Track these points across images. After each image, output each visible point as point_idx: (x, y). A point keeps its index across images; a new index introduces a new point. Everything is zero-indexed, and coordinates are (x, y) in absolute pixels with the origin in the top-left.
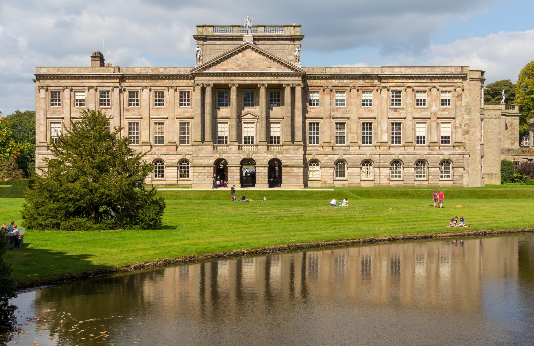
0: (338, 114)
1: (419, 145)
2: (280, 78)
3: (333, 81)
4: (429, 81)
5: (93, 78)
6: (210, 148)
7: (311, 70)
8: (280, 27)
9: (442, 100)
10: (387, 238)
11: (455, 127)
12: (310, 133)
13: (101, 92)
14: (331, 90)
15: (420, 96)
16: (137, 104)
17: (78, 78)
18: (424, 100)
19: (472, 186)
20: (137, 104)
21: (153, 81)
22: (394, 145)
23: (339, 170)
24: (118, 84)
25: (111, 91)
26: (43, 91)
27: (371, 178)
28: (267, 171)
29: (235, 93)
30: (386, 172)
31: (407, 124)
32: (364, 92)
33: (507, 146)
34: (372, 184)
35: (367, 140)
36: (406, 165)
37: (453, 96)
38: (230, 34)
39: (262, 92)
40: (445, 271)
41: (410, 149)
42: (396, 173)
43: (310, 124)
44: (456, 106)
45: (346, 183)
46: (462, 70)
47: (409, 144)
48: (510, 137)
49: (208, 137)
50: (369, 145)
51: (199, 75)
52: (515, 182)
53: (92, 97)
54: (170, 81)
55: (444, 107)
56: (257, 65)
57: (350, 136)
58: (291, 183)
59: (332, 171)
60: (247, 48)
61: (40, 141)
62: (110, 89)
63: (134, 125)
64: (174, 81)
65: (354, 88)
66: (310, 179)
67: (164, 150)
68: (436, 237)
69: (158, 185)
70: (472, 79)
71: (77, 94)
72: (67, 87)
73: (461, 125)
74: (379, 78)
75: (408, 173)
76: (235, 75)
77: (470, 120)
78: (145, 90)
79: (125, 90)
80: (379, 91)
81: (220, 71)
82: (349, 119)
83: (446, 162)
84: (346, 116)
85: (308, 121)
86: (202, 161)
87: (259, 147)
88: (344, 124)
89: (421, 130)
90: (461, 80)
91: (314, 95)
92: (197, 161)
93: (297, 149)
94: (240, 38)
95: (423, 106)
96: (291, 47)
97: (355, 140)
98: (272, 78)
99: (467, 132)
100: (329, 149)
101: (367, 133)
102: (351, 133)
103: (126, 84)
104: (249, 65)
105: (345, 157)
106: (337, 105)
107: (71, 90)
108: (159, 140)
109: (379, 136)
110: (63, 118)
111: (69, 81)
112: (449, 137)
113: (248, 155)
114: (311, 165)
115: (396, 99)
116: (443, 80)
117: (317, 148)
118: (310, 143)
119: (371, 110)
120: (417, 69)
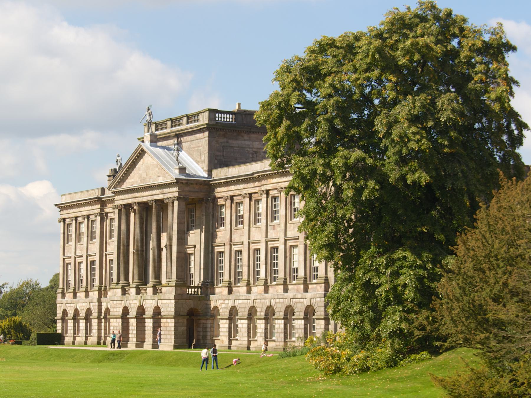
24: (99, 211)
26: (62, 223)
85: (217, 249)
100: (226, 290)
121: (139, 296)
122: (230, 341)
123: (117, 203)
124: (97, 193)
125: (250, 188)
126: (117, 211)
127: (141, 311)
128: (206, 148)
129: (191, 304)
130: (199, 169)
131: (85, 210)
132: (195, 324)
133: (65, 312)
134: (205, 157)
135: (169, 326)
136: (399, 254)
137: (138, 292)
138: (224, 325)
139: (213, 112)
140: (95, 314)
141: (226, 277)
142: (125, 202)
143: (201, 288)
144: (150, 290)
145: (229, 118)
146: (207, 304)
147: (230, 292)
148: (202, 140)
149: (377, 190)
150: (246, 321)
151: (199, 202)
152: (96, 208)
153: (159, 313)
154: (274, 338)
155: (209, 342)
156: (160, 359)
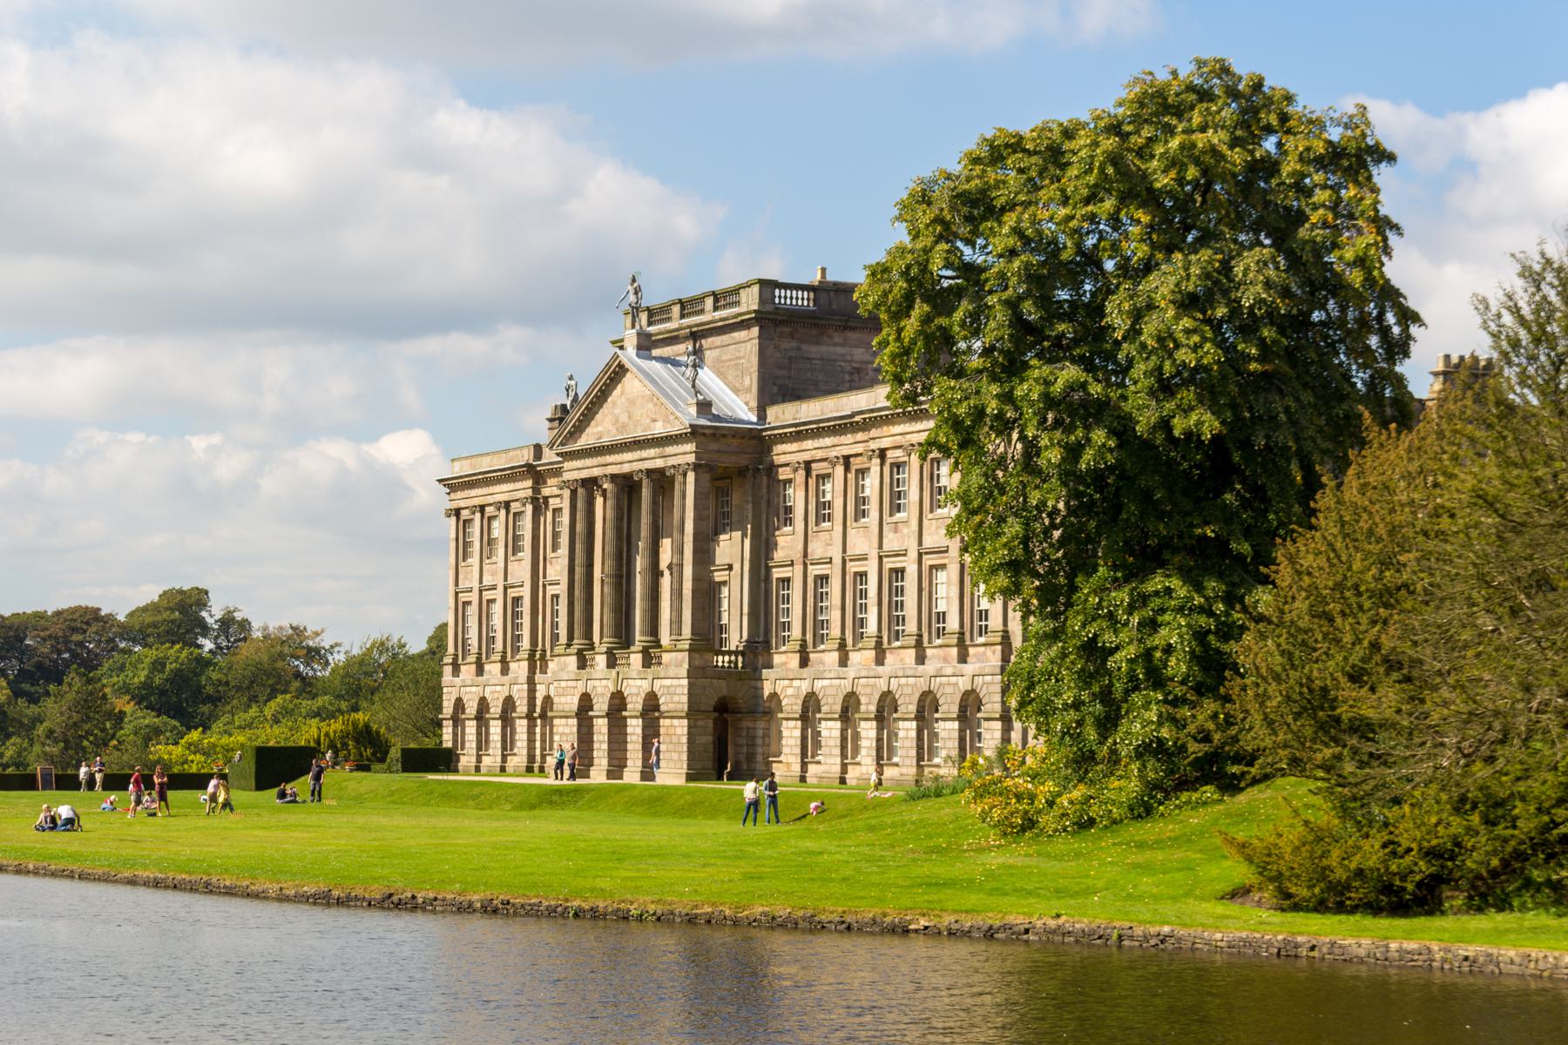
24: (529, 493)
26: (454, 519)
85: (777, 573)
100: (795, 660)
121: (614, 672)
122: (804, 765)
123: (567, 476)
124: (526, 456)
125: (847, 444)
126: (567, 493)
127: (618, 702)
128: (755, 360)
129: (722, 688)
130: (738, 406)
131: (501, 492)
132: (730, 731)
133: (459, 705)
134: (751, 380)
135: (675, 732)
136: (1156, 582)
137: (611, 663)
138: (791, 733)
139: (767, 285)
140: (522, 707)
141: (796, 632)
142: (585, 474)
143: (743, 654)
144: (636, 659)
145: (802, 300)
146: (756, 688)
147: (804, 662)
148: (746, 346)
149: (1111, 450)
150: (838, 724)
151: (738, 474)
152: (524, 487)
153: (657, 708)
154: (895, 760)
155: (760, 767)
156: (657, 803)
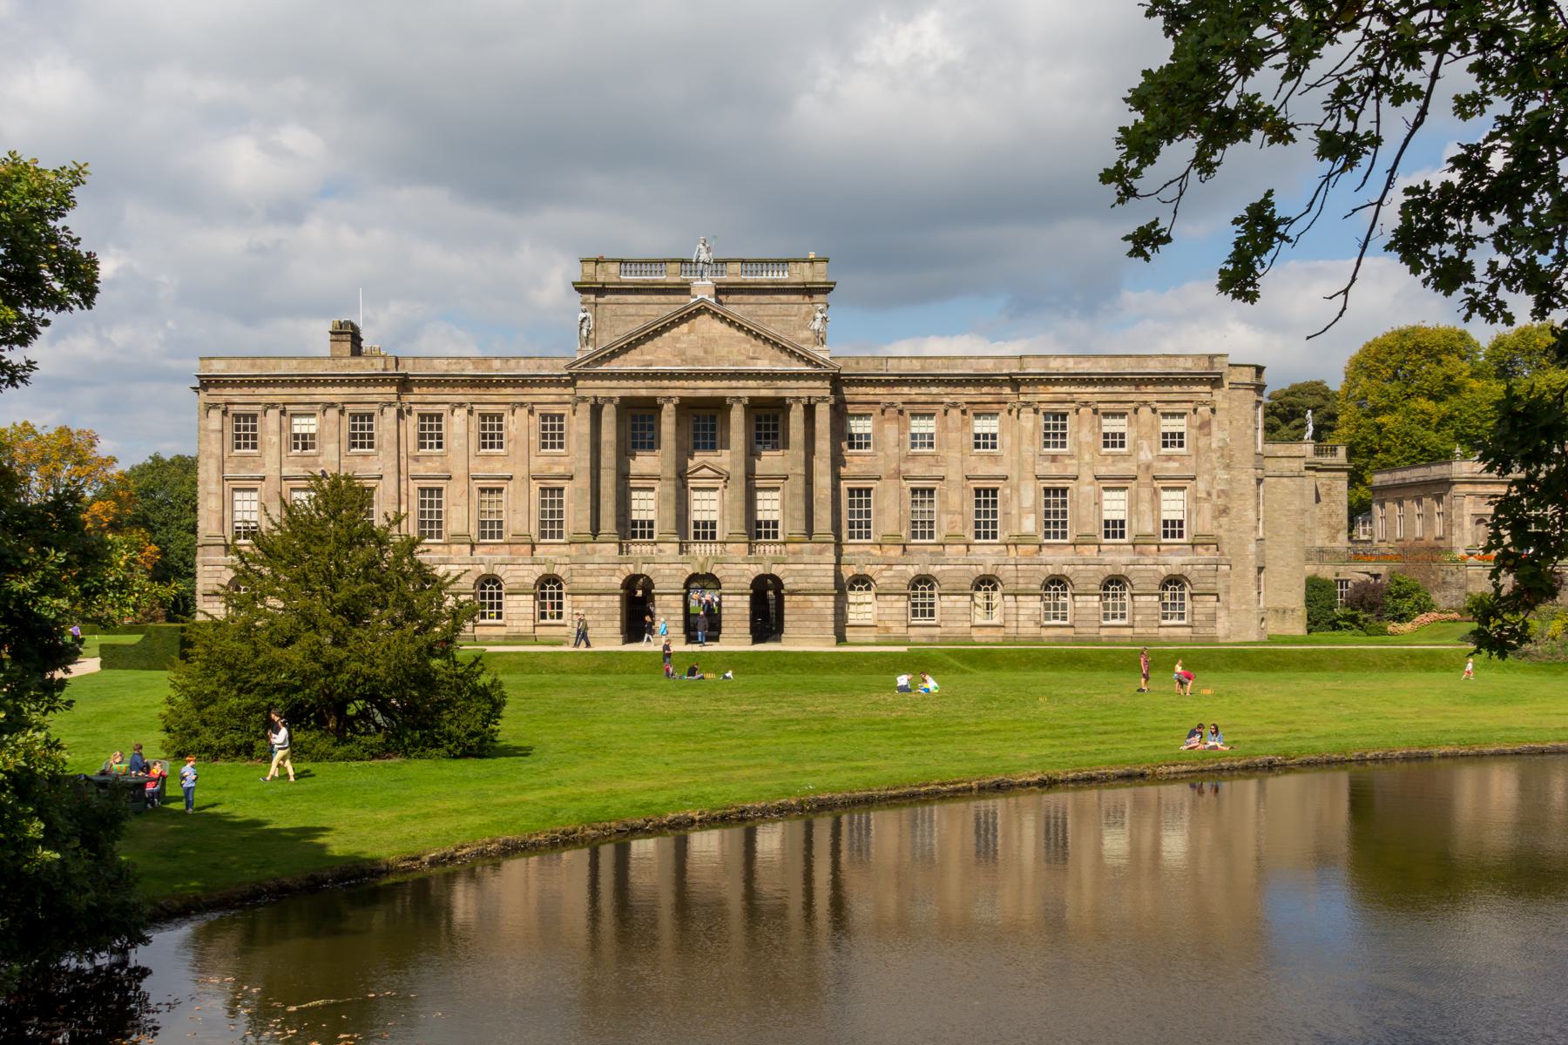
0: (917, 469)
1: (1111, 540)
2: (780, 384)
3: (906, 390)
4: (1133, 389)
5: (334, 384)
6: (611, 549)
7: (852, 363)
8: (779, 262)
9: (1165, 435)
10: (1035, 779)
11: (1196, 500)
12: (851, 514)
13: (354, 416)
14: (901, 412)
15: (1111, 425)
16: (440, 445)
17: (300, 384)
18: (1122, 435)
19: (1238, 639)
20: (440, 445)
21: (477, 391)
22: (1052, 541)
23: (919, 600)
24: (393, 398)
25: (377, 413)
26: (215, 415)
27: (996, 621)
28: (747, 605)
29: (673, 419)
30: (1033, 605)
31: (1083, 491)
32: (977, 416)
33: (1319, 543)
34: (1000, 633)
35: (985, 529)
36: (1081, 588)
37: (1190, 426)
38: (660, 278)
39: (737, 416)
40: (1175, 844)
41: (1090, 552)
42: (1056, 608)
43: (851, 491)
44: (1197, 449)
45: (937, 630)
46: (1211, 362)
47: (1085, 539)
48: (1326, 520)
49: (608, 523)
50: (990, 541)
51: (587, 376)
52: (1340, 628)
53: (331, 429)
54: (518, 390)
55: (1169, 450)
56: (724, 351)
57: (945, 519)
58: (805, 634)
59: (903, 604)
60: (699, 312)
61: (209, 532)
62: (375, 408)
63: (430, 495)
64: (527, 390)
65: (955, 405)
66: (850, 622)
67: (503, 554)
68: (1154, 774)
69: (489, 637)
70: (1235, 386)
71: (296, 421)
72: (273, 405)
73: (1209, 494)
74: (1015, 382)
75: (1085, 606)
76: (672, 376)
77: (1230, 482)
78: (457, 411)
79: (409, 412)
80: (1014, 413)
81: (635, 368)
82: (943, 479)
83: (1174, 581)
84: (936, 472)
85: (844, 485)
86: (593, 580)
87: (729, 547)
88: (931, 491)
89: (1115, 506)
90: (1208, 389)
91: (860, 423)
92: (581, 579)
93: (820, 553)
94: (684, 289)
95: (1118, 450)
96: (805, 308)
97: (958, 531)
98: (761, 383)
99: (1225, 511)
101: (986, 513)
102: (948, 512)
103: (412, 398)
104: (706, 352)
105: (934, 570)
106: (914, 445)
107: (283, 413)
108: (490, 529)
109: (1015, 521)
110: (263, 479)
111: (278, 390)
112: (1181, 523)
113: (702, 566)
114: (852, 588)
115: (1055, 429)
116: (1166, 388)
117: (868, 548)
118: (851, 536)
119: (995, 459)
120: (1104, 362)
